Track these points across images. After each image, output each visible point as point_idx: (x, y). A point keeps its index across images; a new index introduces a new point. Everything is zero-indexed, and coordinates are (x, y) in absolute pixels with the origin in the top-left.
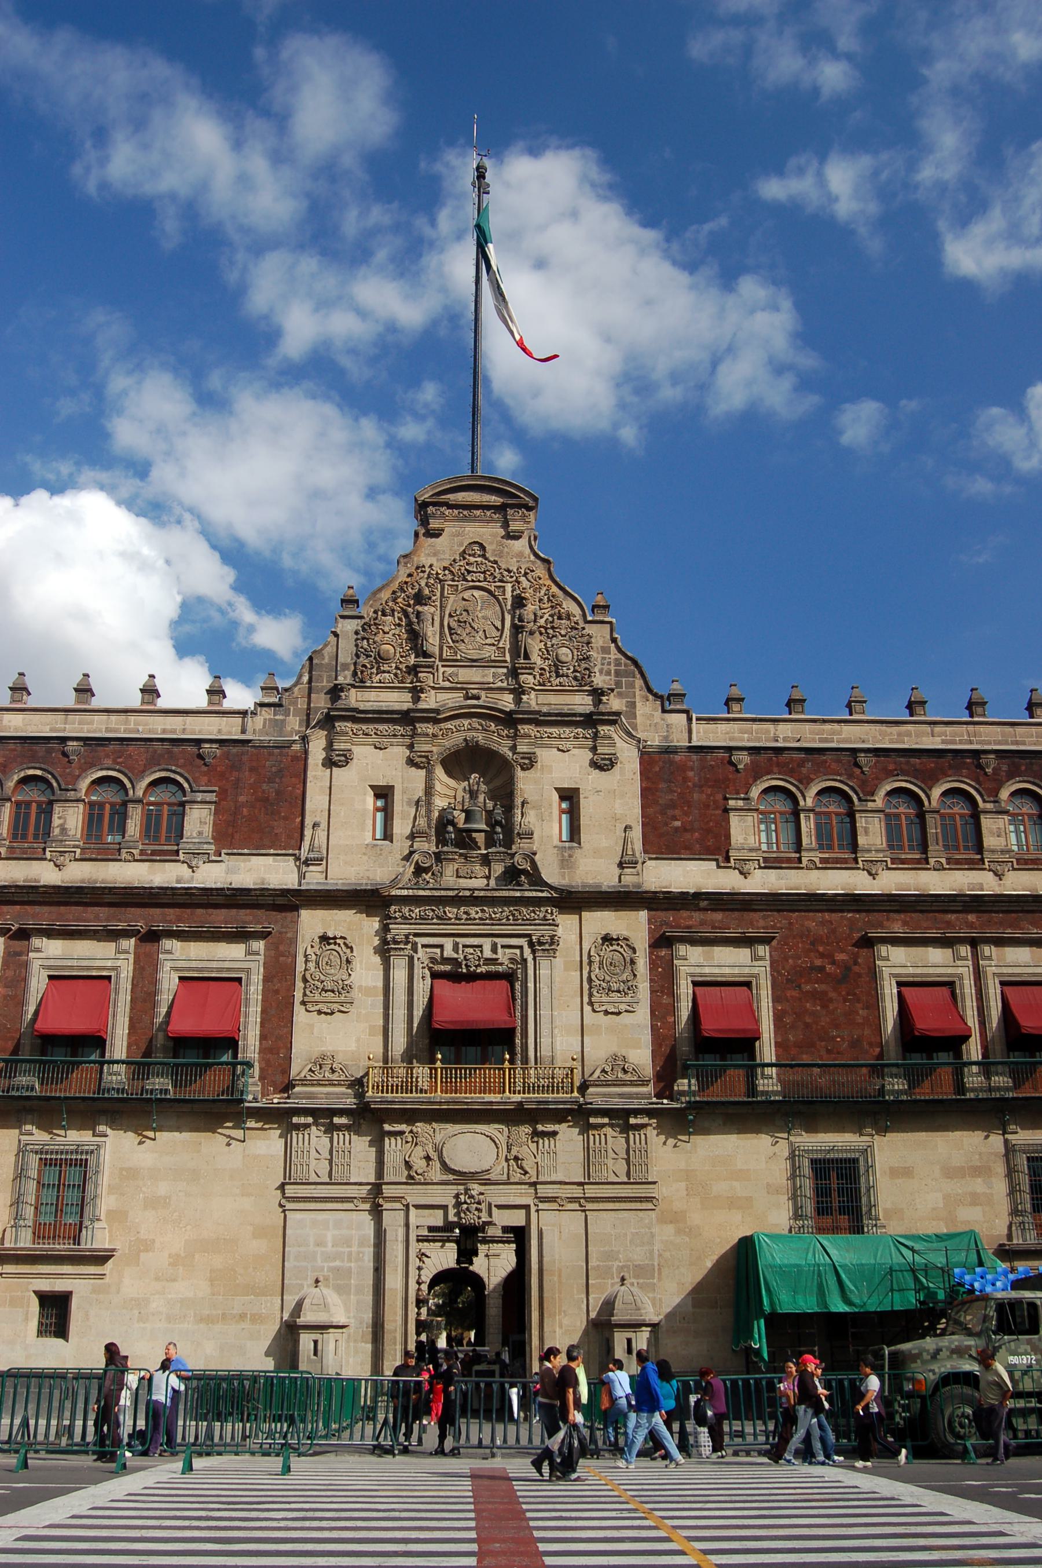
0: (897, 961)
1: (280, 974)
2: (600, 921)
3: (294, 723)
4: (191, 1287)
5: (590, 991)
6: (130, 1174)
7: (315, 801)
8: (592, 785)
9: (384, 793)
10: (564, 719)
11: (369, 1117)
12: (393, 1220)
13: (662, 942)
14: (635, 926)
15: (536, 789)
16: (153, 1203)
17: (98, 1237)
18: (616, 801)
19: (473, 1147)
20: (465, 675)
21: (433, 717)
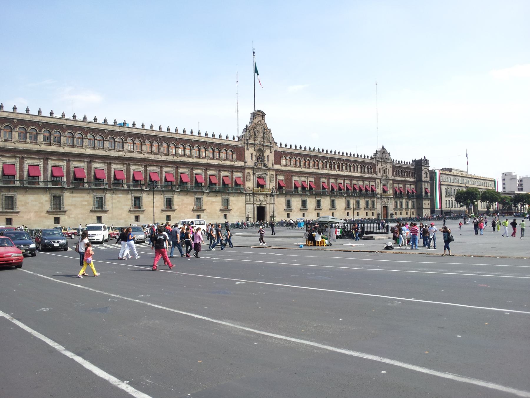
0: (295, 178)
1: (244, 177)
2: (271, 172)
3: (243, 144)
4: (238, 213)
5: (271, 180)
6: (232, 200)
7: (246, 155)
8: (270, 154)
9: (252, 154)
10: (268, 146)
11: (254, 194)
12: (255, 206)
13: (276, 175)
14: (274, 173)
15: (265, 155)
16: (234, 204)
17: (230, 208)
18: (272, 157)
19: (262, 198)
20: (259, 139)
21: (257, 144)
